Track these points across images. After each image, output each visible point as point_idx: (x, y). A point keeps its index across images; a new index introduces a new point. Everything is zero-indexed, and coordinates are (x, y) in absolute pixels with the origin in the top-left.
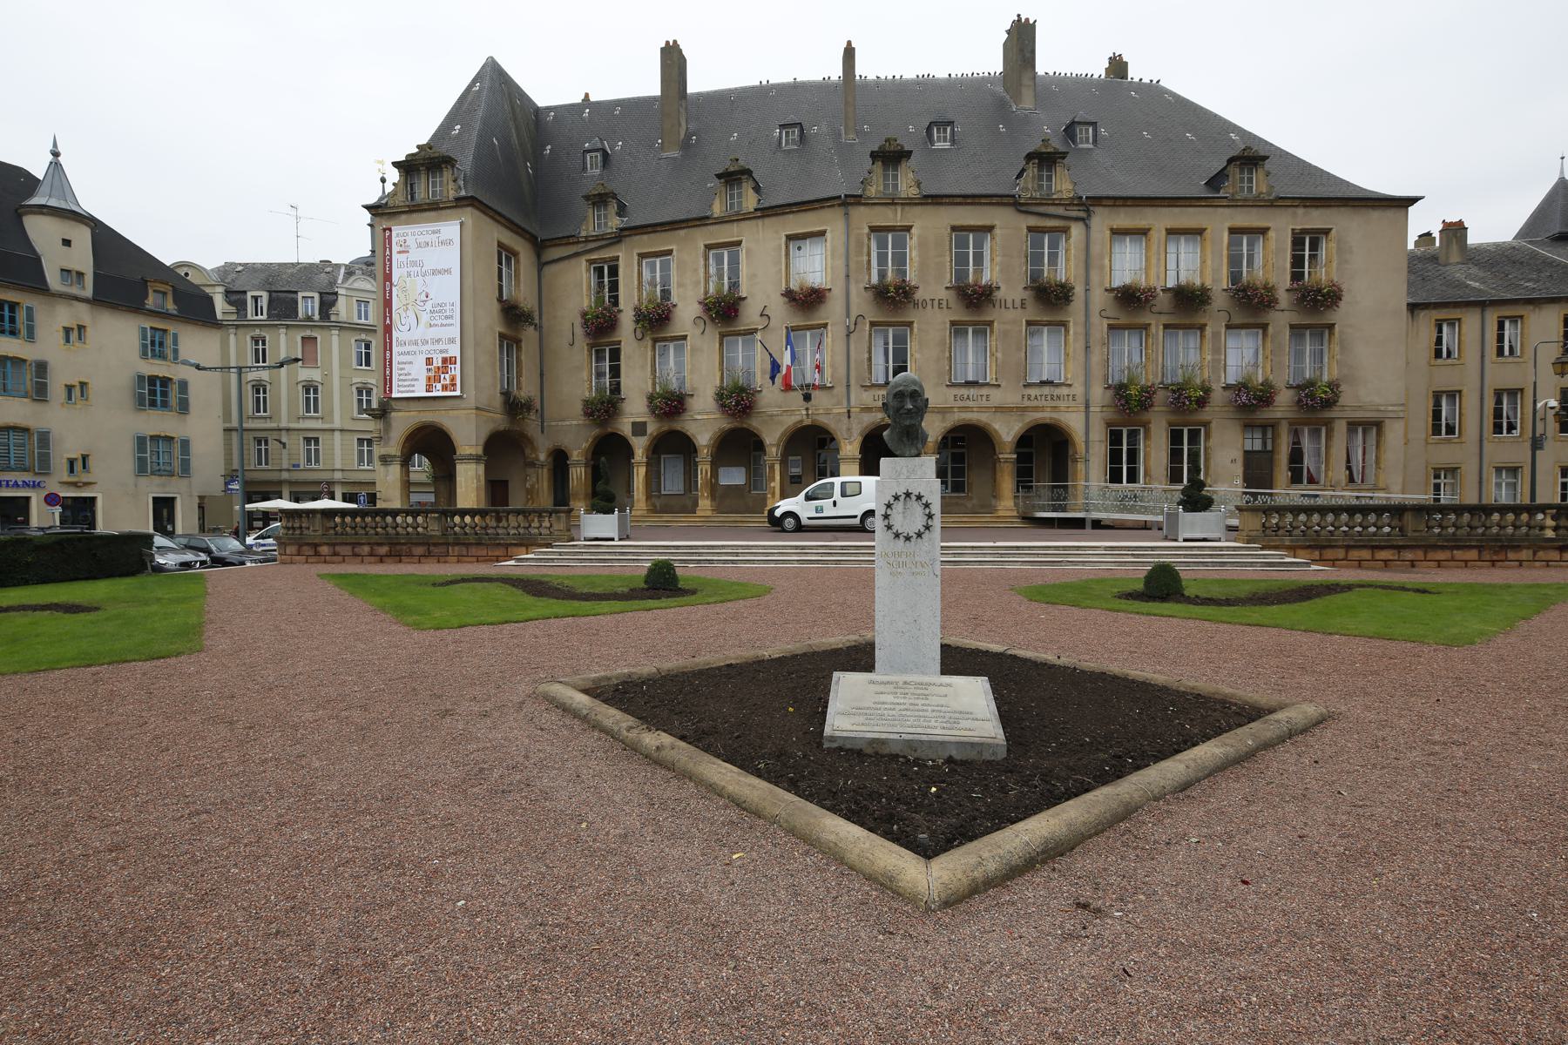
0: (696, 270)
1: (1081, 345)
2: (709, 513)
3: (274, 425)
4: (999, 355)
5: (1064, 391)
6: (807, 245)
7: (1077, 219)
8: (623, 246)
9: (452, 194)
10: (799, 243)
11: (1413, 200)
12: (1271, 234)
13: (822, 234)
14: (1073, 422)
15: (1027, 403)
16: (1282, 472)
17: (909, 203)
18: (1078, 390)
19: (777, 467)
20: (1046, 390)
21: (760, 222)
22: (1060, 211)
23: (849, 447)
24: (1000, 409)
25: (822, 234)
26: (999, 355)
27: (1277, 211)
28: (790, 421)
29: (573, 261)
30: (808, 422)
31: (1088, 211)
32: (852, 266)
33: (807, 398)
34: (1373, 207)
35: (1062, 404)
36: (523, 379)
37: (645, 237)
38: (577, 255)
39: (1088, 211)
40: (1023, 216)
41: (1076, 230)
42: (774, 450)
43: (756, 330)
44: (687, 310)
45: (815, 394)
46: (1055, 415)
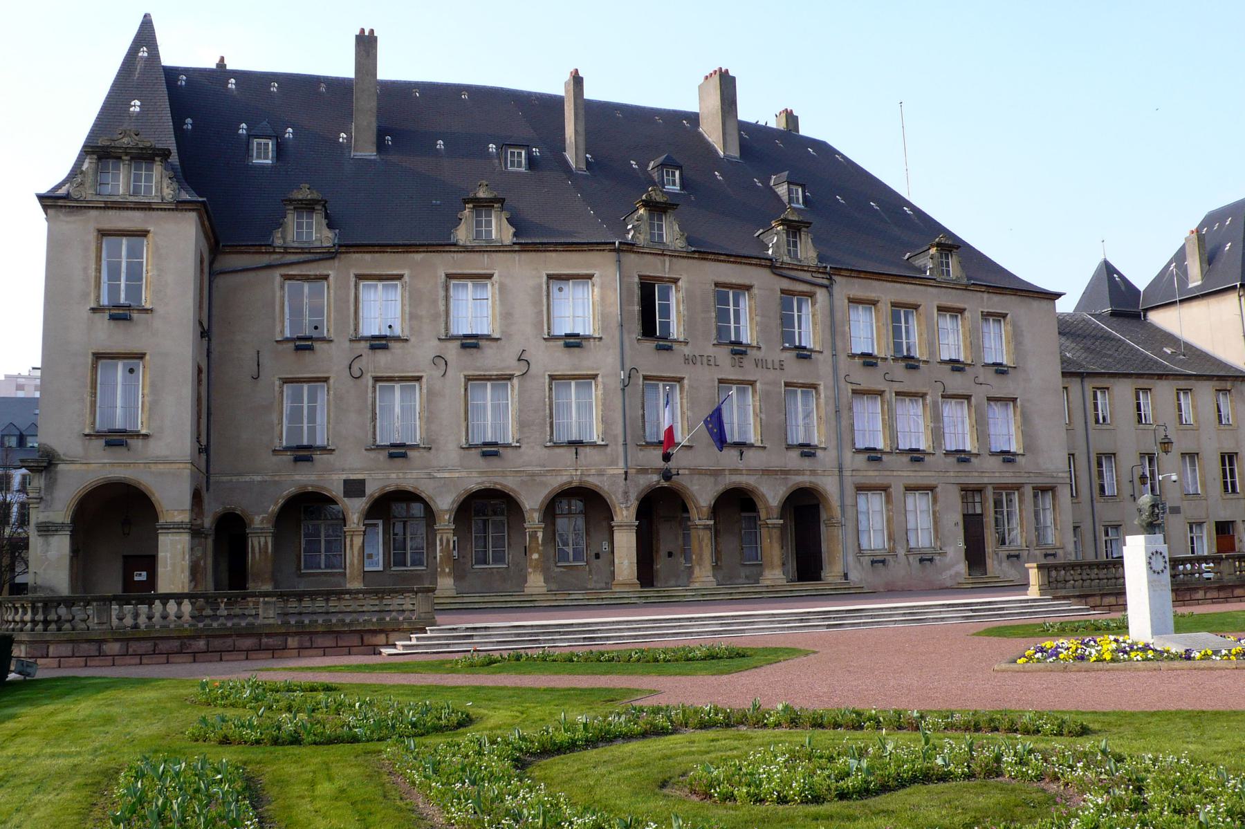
0: (435, 302)
1: (831, 408)
4: (763, 416)
6: (569, 287)
10: (562, 284)
12: (967, 314)
14: (829, 486)
17: (675, 255)
21: (516, 256)
22: (808, 276)
24: (766, 472)
25: (590, 277)
26: (763, 416)
27: (970, 294)
29: (263, 274)
31: (830, 279)
37: (368, 257)
39: (830, 279)
41: (821, 295)
43: (510, 378)
46: (813, 479)
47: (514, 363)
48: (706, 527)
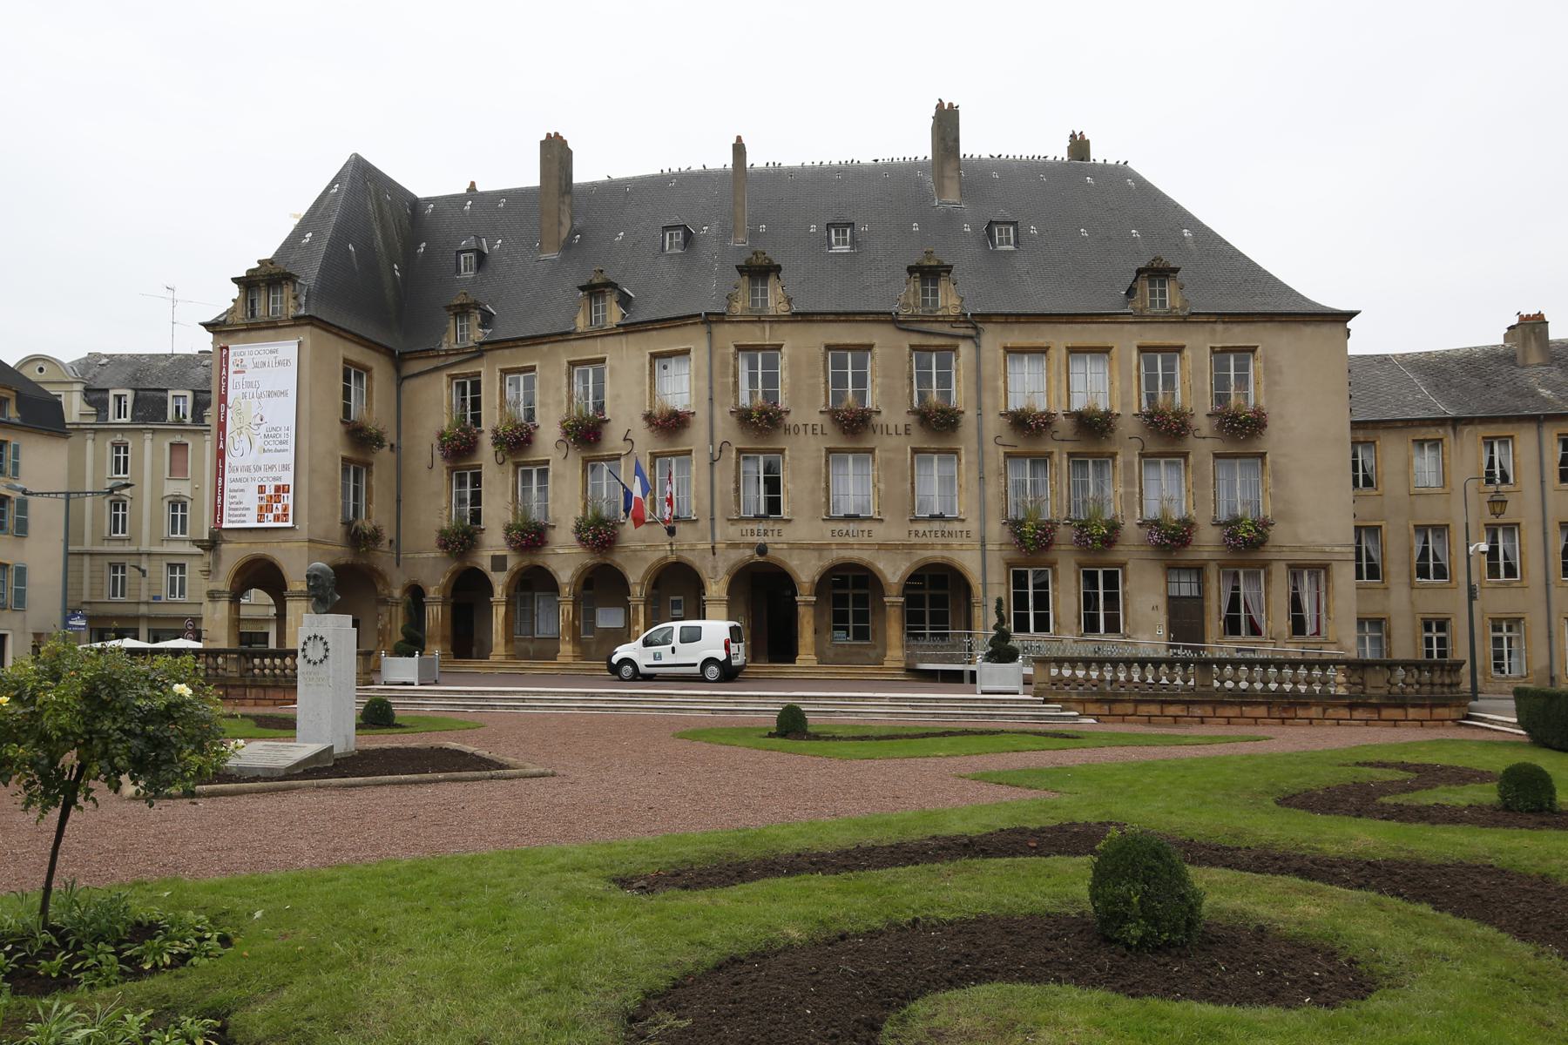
0: (559, 389)
1: (974, 474)
2: (570, 660)
3: (133, 548)
4: (882, 486)
5: (957, 526)
6: (673, 364)
7: (965, 337)
8: (485, 361)
9: (292, 312)
10: (665, 362)
11: (1352, 315)
12: (1187, 352)
13: (687, 352)
14: (968, 562)
15: (914, 540)
16: (1214, 624)
17: (778, 320)
18: (973, 525)
19: (641, 608)
20: (936, 526)
21: (623, 338)
22: (946, 328)
23: (714, 588)
24: (883, 547)
25: (687, 352)
26: (882, 486)
27: (1192, 327)
28: (654, 557)
29: (434, 376)
30: (672, 559)
32: (716, 387)
33: (671, 532)
34: (1304, 322)
35: (954, 541)
36: (373, 507)
37: (507, 352)
38: (437, 369)
39: (975, 328)
40: (903, 335)
41: (965, 349)
42: (638, 589)
44: (549, 434)
45: (680, 527)
46: (947, 554)
47: (621, 443)
48: (807, 604)
